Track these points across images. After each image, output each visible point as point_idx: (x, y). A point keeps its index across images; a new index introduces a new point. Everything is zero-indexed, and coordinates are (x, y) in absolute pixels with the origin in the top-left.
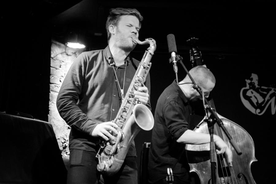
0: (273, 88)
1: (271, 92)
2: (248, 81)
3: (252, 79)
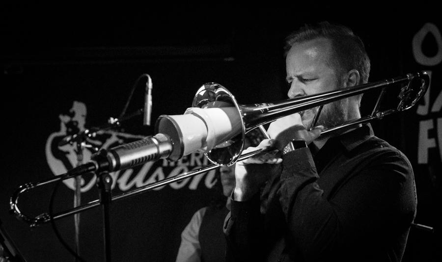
0: (115, 131)
2: (65, 119)
3: (72, 115)
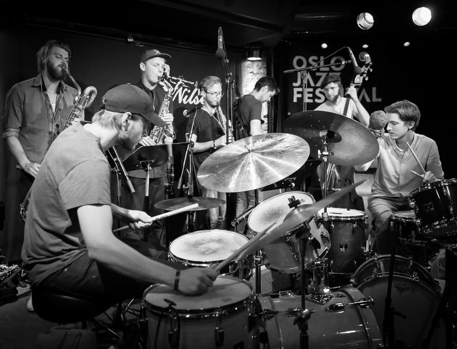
1: (179, 83)
